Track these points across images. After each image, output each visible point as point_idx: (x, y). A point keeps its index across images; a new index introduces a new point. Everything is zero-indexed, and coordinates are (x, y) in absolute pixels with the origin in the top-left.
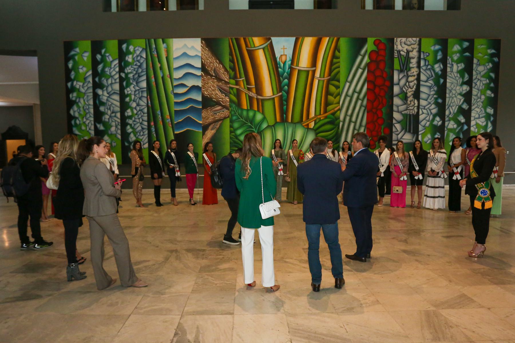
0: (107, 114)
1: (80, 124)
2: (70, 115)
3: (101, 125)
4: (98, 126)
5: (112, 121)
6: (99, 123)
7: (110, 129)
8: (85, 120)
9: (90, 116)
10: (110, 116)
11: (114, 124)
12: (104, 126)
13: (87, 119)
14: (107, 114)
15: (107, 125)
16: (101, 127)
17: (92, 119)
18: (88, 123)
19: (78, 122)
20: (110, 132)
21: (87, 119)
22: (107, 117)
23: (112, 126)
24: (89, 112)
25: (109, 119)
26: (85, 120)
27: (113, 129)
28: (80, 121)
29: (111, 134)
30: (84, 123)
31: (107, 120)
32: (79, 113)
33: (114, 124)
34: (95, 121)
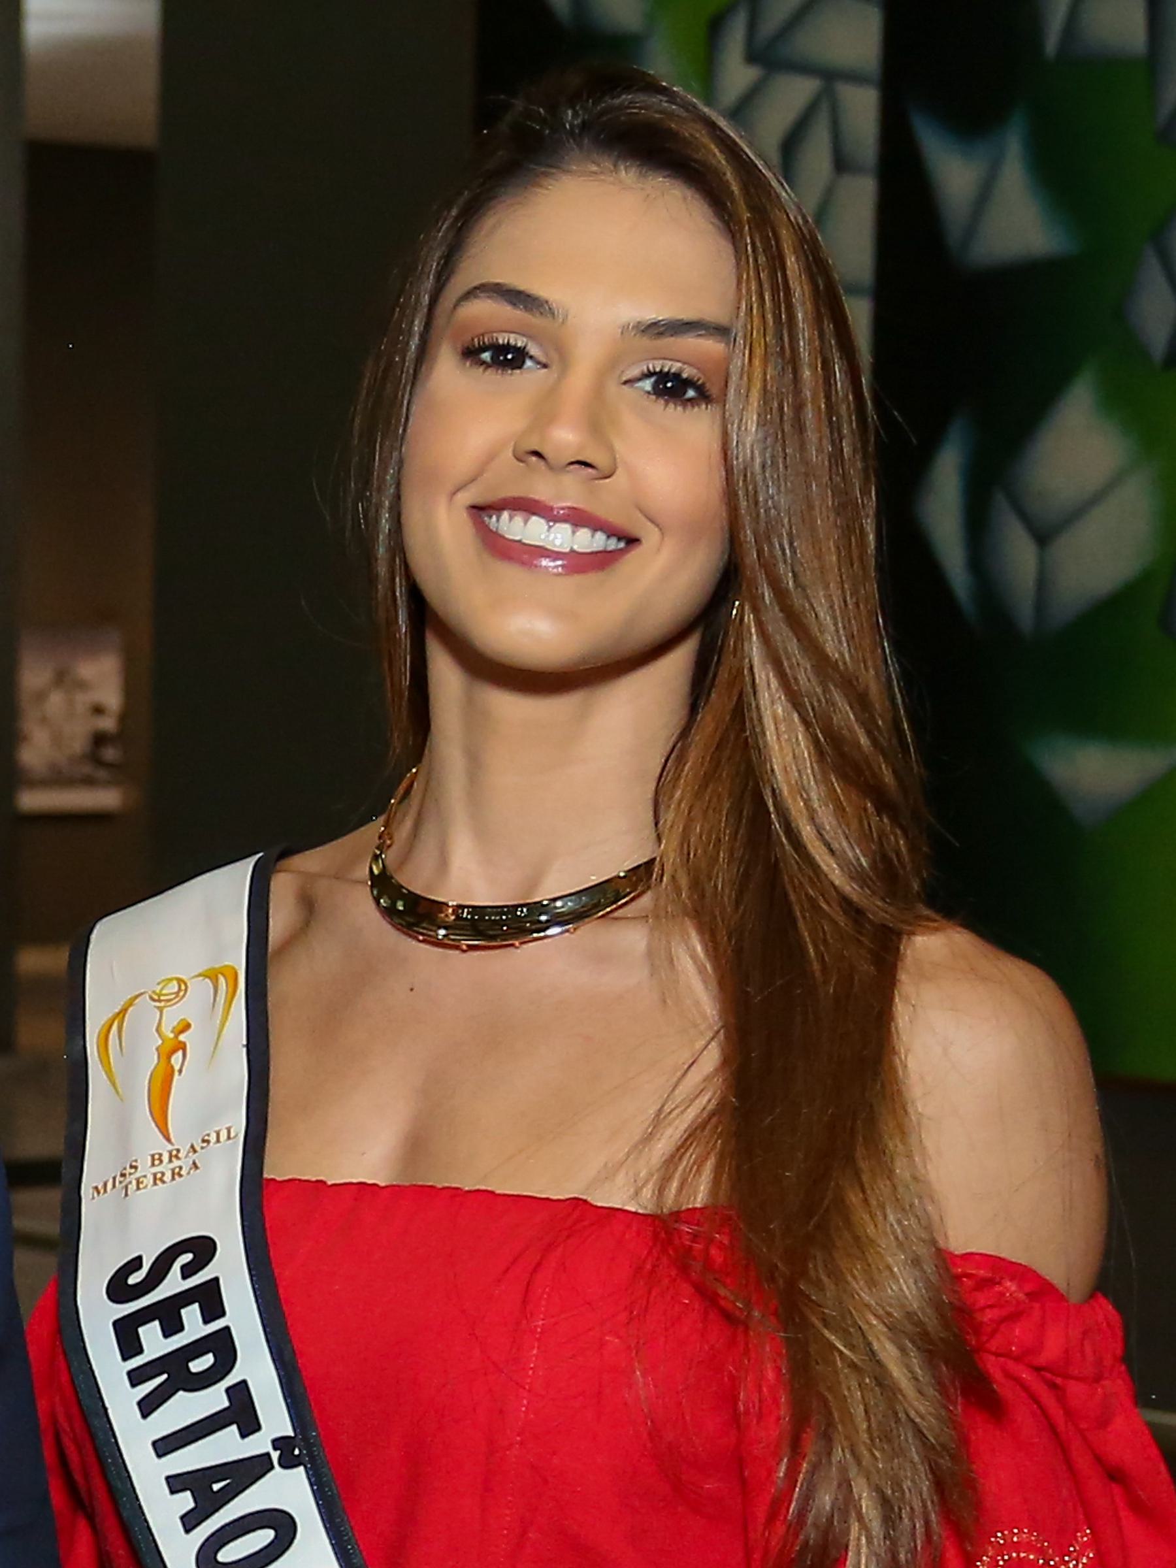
3: (1014, 175)
12: (1062, 176)
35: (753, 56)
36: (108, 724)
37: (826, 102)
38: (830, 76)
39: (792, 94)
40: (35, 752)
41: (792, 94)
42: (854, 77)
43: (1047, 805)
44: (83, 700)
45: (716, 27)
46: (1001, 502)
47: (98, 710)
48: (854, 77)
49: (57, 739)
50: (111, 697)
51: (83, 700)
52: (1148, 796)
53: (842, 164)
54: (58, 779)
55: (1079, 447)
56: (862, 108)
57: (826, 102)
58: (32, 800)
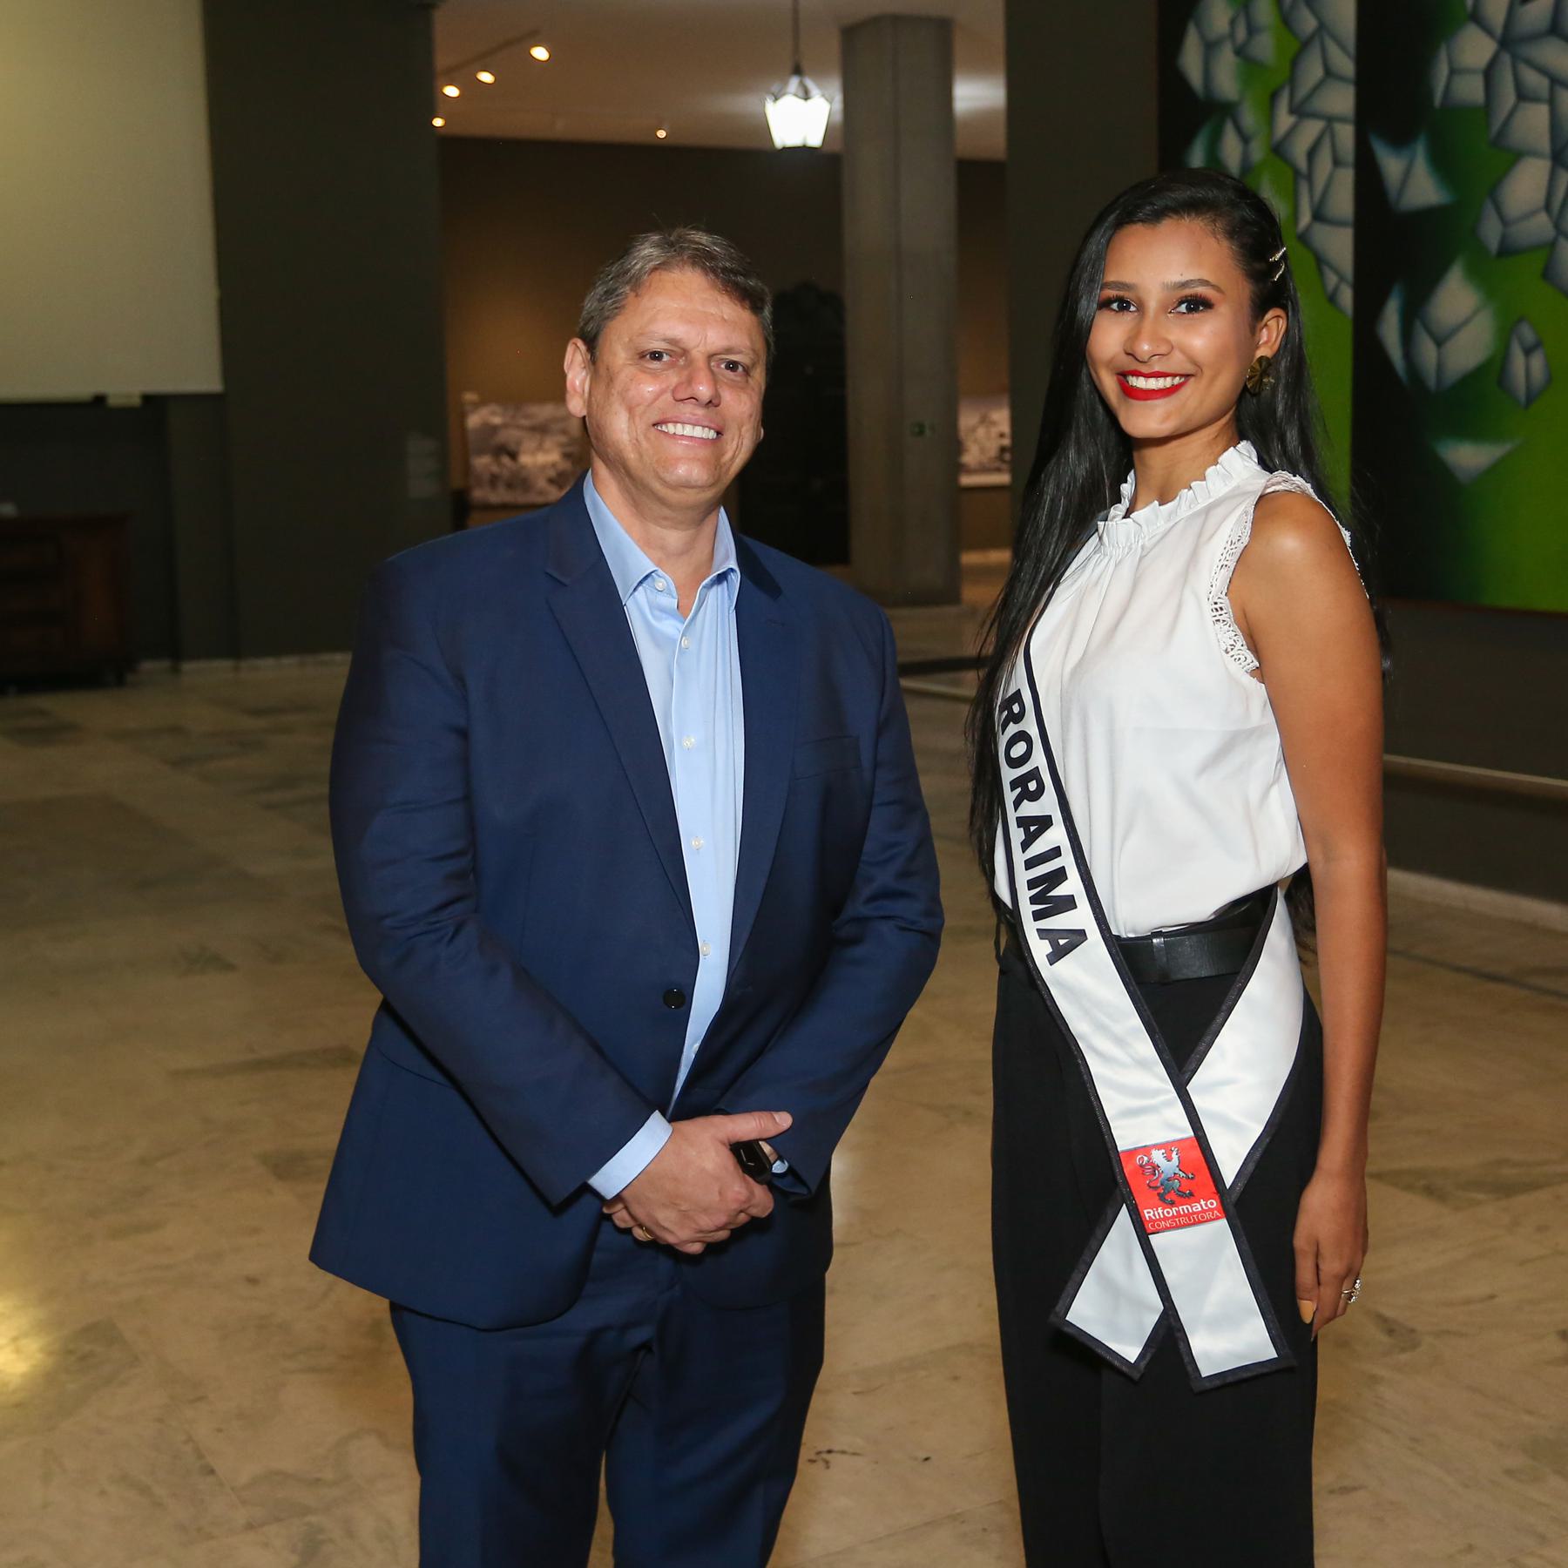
0: (1476, 18)
1: (1246, 167)
2: (1181, 80)
4: (1391, 165)
5: (1523, 96)
6: (1400, 139)
7: (1494, 193)
8: (1284, 120)
9: (1329, 73)
10: (1509, 41)
11: (1533, 124)
12: (1443, 164)
13: (1301, 111)
14: (1476, 18)
15: (1470, 150)
16: (1415, 182)
17: (1342, 100)
18: (1312, 154)
19: (1232, 151)
20: (1491, 232)
21: (1301, 111)
22: (1475, 48)
23: (1517, 155)
24: (1322, 28)
25: (1489, 73)
26: (1284, 120)
27: (1527, 185)
28: (1245, 139)
29: (1507, 250)
30: (1279, 150)
31: (1471, 90)
32: (1240, 52)
33: (1533, 124)
34: (1368, 118)
35: (1293, 110)
36: (1006, 442)
37: (1329, 131)
38: (1330, 120)
39: (1311, 130)
40: (971, 457)
41: (1312, 129)
42: (1342, 120)
43: (1444, 473)
44: (994, 431)
45: (1274, 97)
46: (1418, 324)
47: (1002, 435)
48: (1342, 120)
49: (982, 450)
50: (1005, 427)
51: (994, 431)
52: (1494, 468)
53: (1337, 162)
54: (983, 469)
55: (1456, 297)
56: (1346, 134)
57: (1329, 131)
58: (966, 480)
